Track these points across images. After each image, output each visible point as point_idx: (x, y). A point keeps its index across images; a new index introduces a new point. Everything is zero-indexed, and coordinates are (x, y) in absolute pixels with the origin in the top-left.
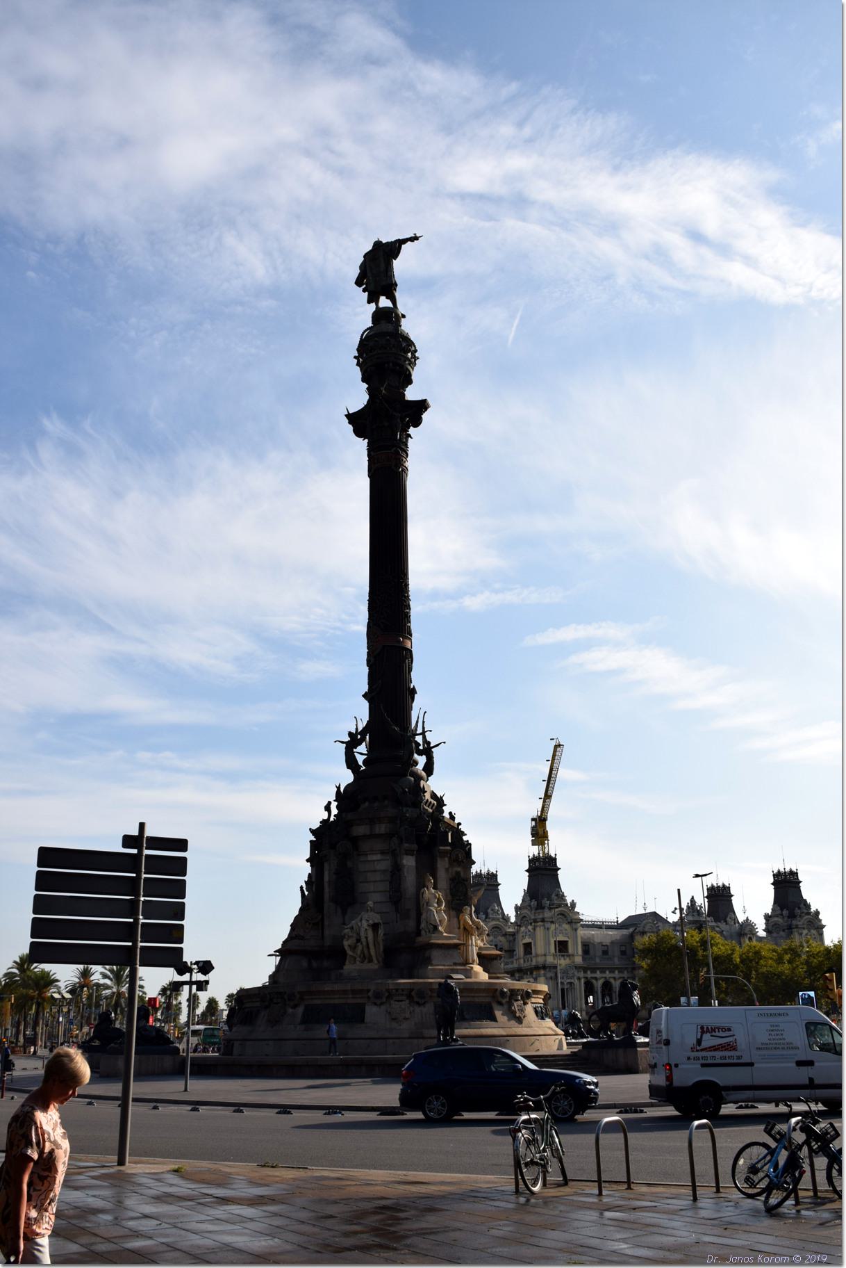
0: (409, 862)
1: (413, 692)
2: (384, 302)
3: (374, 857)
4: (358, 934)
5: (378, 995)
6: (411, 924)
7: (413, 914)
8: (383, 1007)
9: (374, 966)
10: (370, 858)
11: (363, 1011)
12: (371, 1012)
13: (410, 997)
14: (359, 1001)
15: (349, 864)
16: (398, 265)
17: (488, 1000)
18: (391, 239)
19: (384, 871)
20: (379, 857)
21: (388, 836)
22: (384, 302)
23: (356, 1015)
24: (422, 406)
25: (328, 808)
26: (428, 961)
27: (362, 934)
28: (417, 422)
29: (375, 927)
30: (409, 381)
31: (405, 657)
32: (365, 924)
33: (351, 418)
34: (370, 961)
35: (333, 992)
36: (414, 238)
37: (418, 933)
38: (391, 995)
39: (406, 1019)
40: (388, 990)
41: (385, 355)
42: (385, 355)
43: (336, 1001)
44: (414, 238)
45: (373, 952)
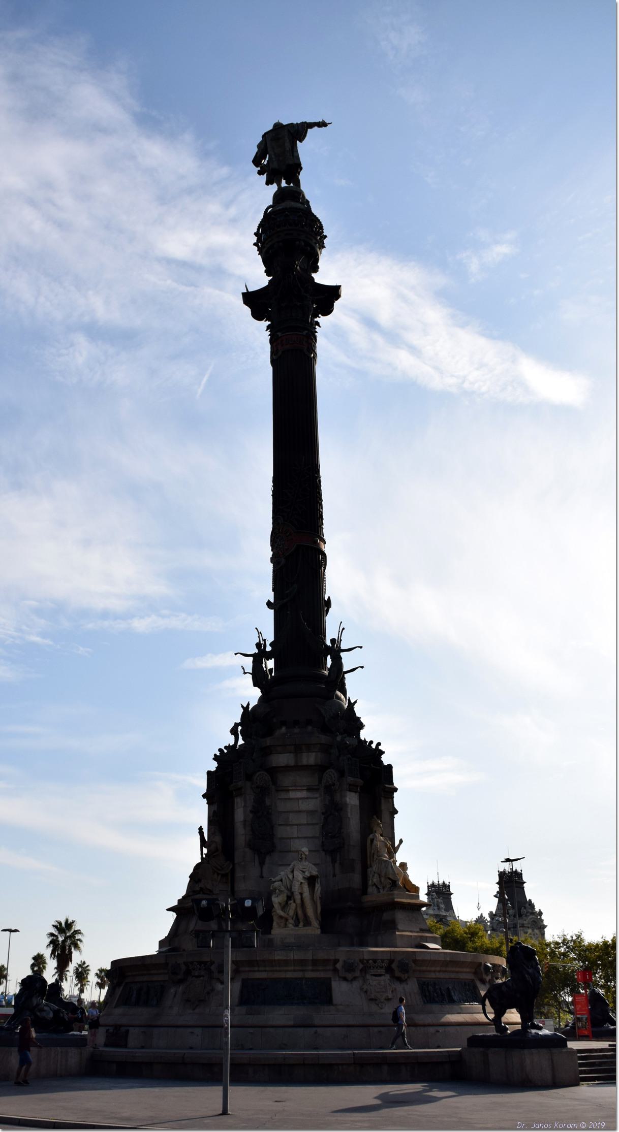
0: (352, 800)
1: (328, 603)
3: (299, 795)
4: (290, 889)
5: (349, 967)
6: (357, 878)
7: (358, 867)
8: (356, 984)
9: (315, 929)
10: (292, 795)
11: (329, 989)
12: (340, 989)
13: (389, 970)
14: (322, 975)
15: (268, 802)
16: (304, 149)
17: (470, 976)
19: (311, 813)
20: (304, 794)
21: (320, 769)
23: (321, 995)
24: (333, 293)
25: (234, 731)
26: (392, 926)
27: (296, 889)
28: (328, 310)
29: (311, 880)
30: (316, 269)
31: (318, 561)
32: (299, 876)
33: (250, 298)
34: (307, 923)
35: (286, 962)
36: (323, 124)
37: (364, 890)
38: (368, 966)
39: (388, 1000)
40: (362, 961)
41: (290, 237)
42: (290, 237)
43: (289, 975)
44: (323, 124)
45: (310, 912)
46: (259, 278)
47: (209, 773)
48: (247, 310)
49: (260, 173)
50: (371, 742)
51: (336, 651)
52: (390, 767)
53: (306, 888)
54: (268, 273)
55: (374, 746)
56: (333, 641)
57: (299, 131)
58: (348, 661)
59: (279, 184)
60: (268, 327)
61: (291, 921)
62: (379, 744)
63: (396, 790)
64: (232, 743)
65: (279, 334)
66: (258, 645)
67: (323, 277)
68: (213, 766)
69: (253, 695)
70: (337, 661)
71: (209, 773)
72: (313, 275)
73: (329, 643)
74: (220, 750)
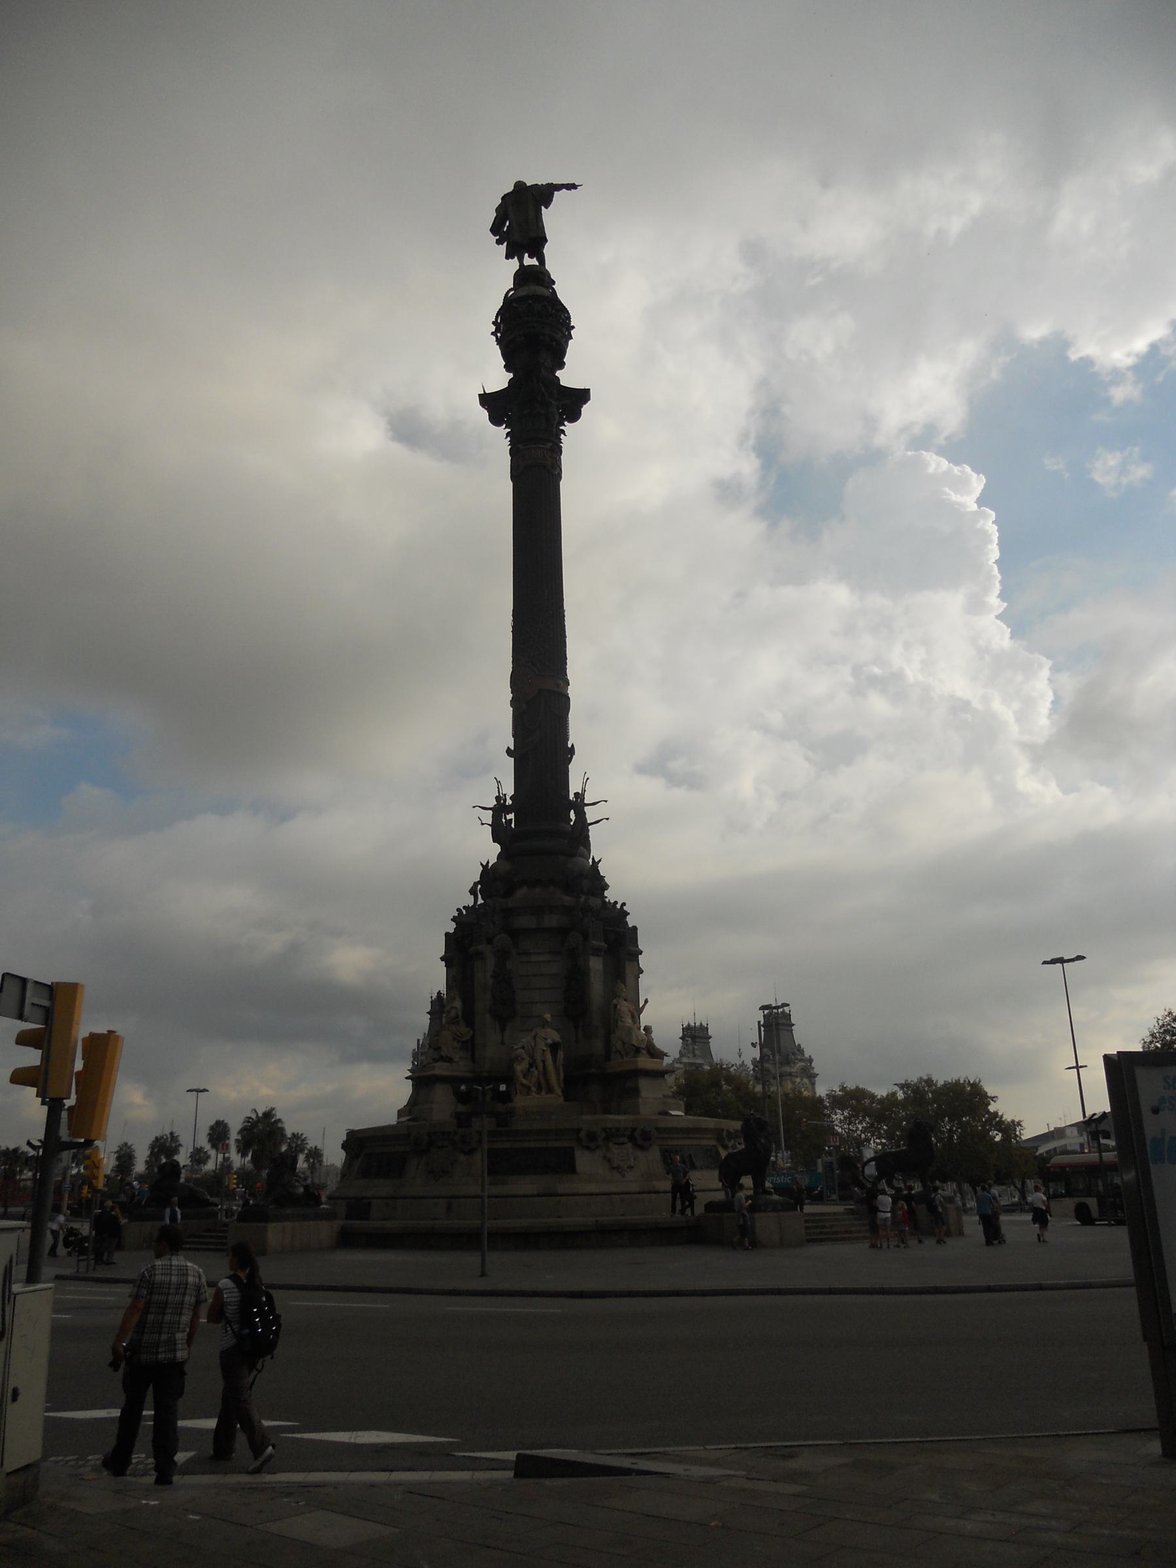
1: (572, 751)
2: (529, 261)
3: (541, 958)
4: (532, 1057)
5: (592, 1136)
9: (556, 1098)
10: (533, 958)
11: (573, 1158)
12: (584, 1160)
13: (632, 1138)
16: (550, 217)
17: (713, 1143)
18: (542, 181)
22: (529, 261)
23: (565, 1164)
24: (583, 396)
25: (473, 892)
26: (636, 1092)
27: (538, 1056)
28: (574, 416)
29: (554, 1047)
30: (561, 365)
32: (542, 1045)
33: (486, 400)
34: (550, 1090)
36: (572, 186)
37: (608, 1058)
38: (612, 1135)
39: (631, 1167)
40: (604, 1130)
41: (533, 326)
42: (533, 326)
44: (572, 186)
46: (498, 378)
47: (447, 934)
48: (485, 414)
49: (499, 242)
50: (616, 903)
51: (579, 804)
52: (635, 928)
53: (549, 1057)
54: (508, 368)
55: (618, 906)
56: (576, 794)
57: (543, 194)
58: (591, 814)
59: (521, 260)
60: (508, 435)
61: (534, 1089)
62: (624, 904)
63: (641, 952)
64: (471, 904)
65: (521, 446)
66: (498, 798)
67: (568, 377)
68: (451, 927)
69: (491, 852)
70: (581, 815)
71: (447, 934)
72: (558, 373)
73: (572, 796)
74: (458, 910)
